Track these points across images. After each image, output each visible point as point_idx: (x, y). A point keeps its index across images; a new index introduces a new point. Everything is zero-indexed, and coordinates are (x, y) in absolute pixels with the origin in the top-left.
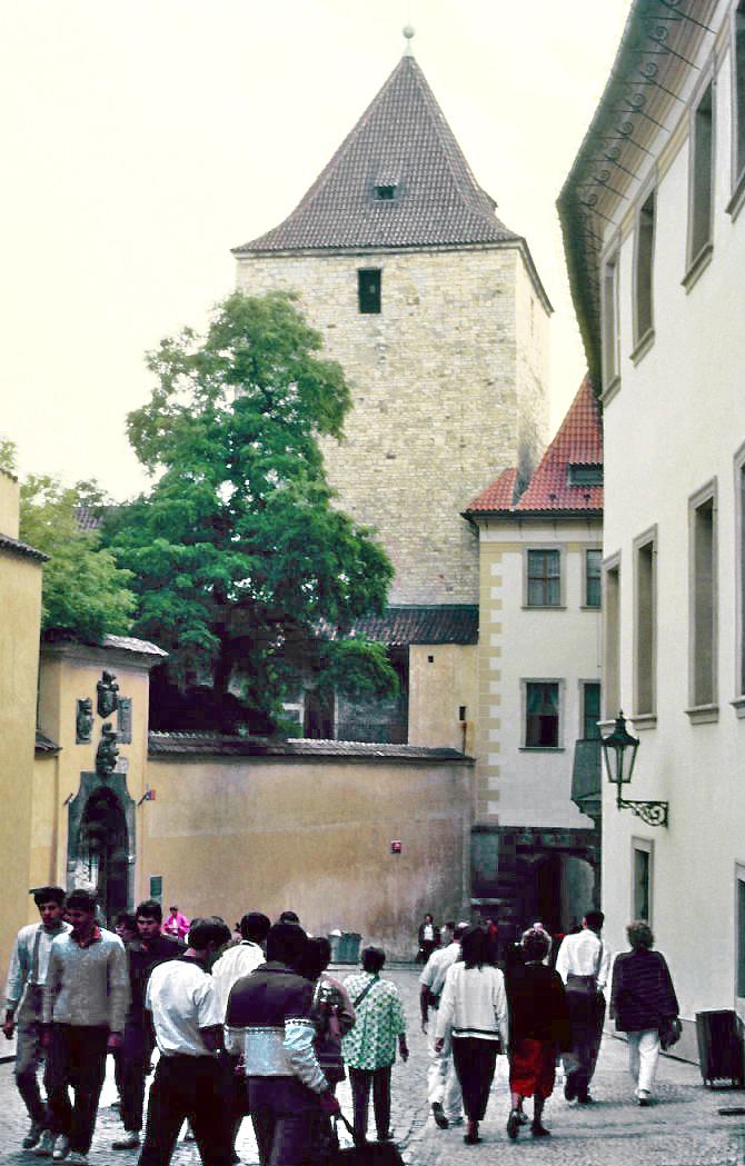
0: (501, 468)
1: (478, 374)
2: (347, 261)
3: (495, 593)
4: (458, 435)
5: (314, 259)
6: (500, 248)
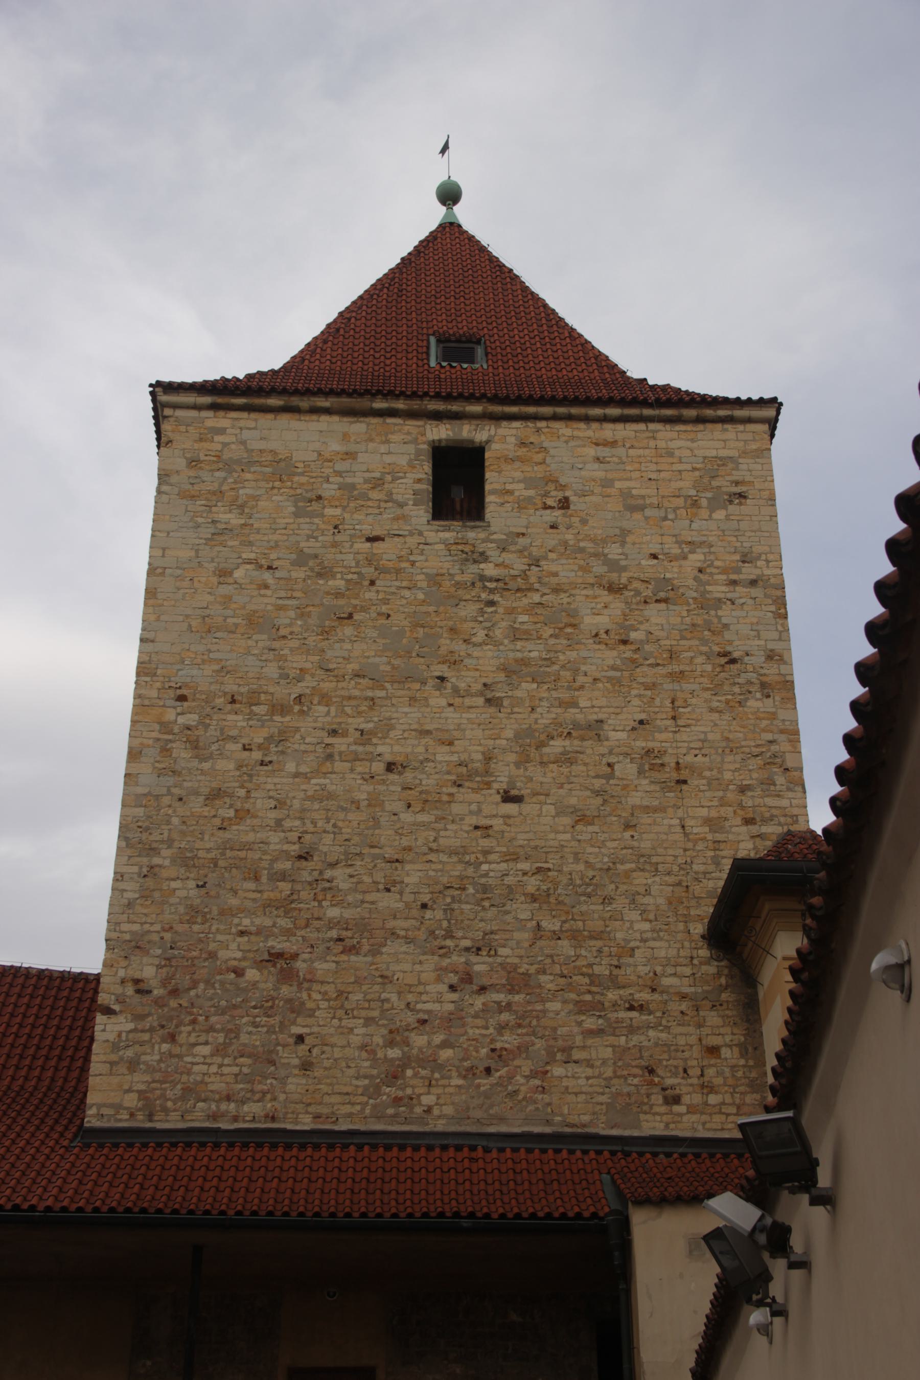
0: (774, 830)
1: (704, 642)
2: (412, 426)
4: (670, 760)
5: (336, 418)
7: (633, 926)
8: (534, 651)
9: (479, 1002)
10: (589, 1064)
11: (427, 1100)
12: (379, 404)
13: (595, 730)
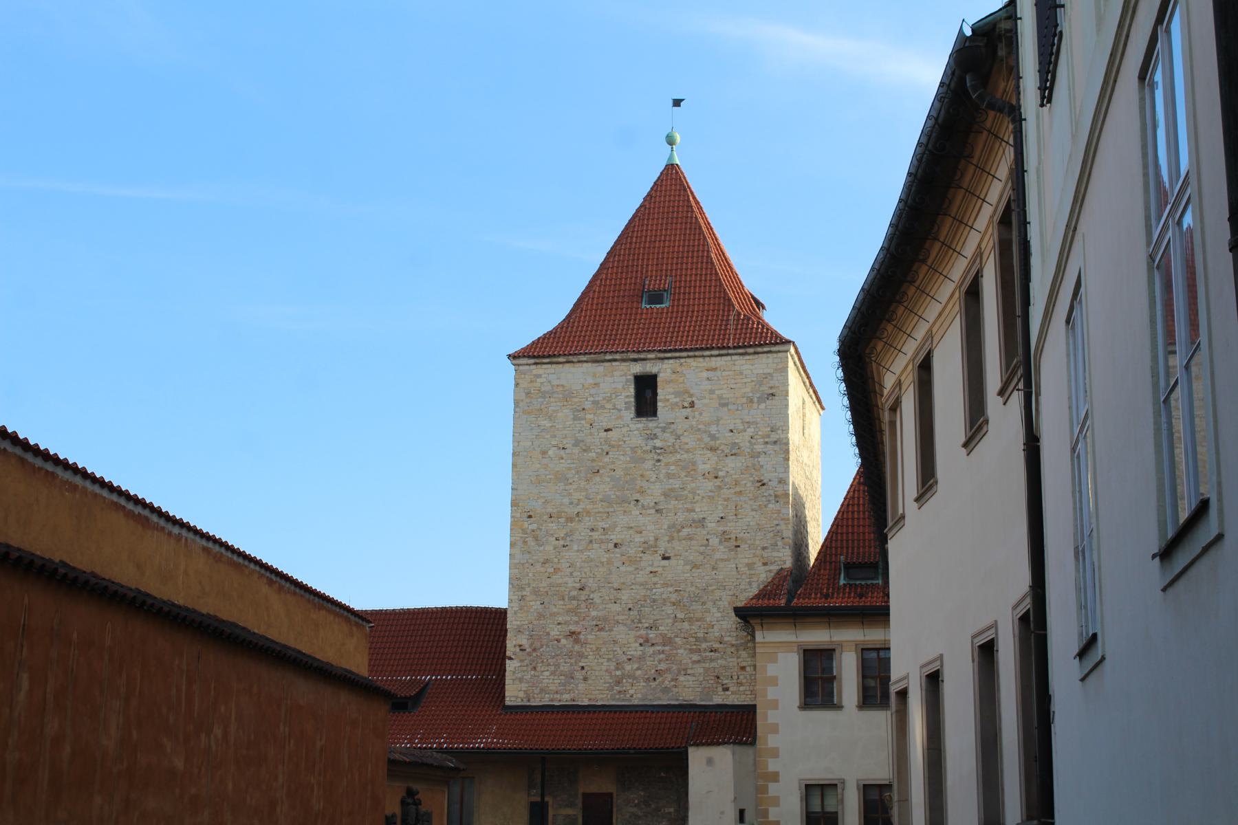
0: (775, 568)
1: (752, 475)
3: (771, 693)
6: (770, 352)
7: (714, 615)
8: (676, 484)
9: (651, 650)
10: (694, 675)
11: (631, 692)
12: (608, 357)
13: (702, 522)
